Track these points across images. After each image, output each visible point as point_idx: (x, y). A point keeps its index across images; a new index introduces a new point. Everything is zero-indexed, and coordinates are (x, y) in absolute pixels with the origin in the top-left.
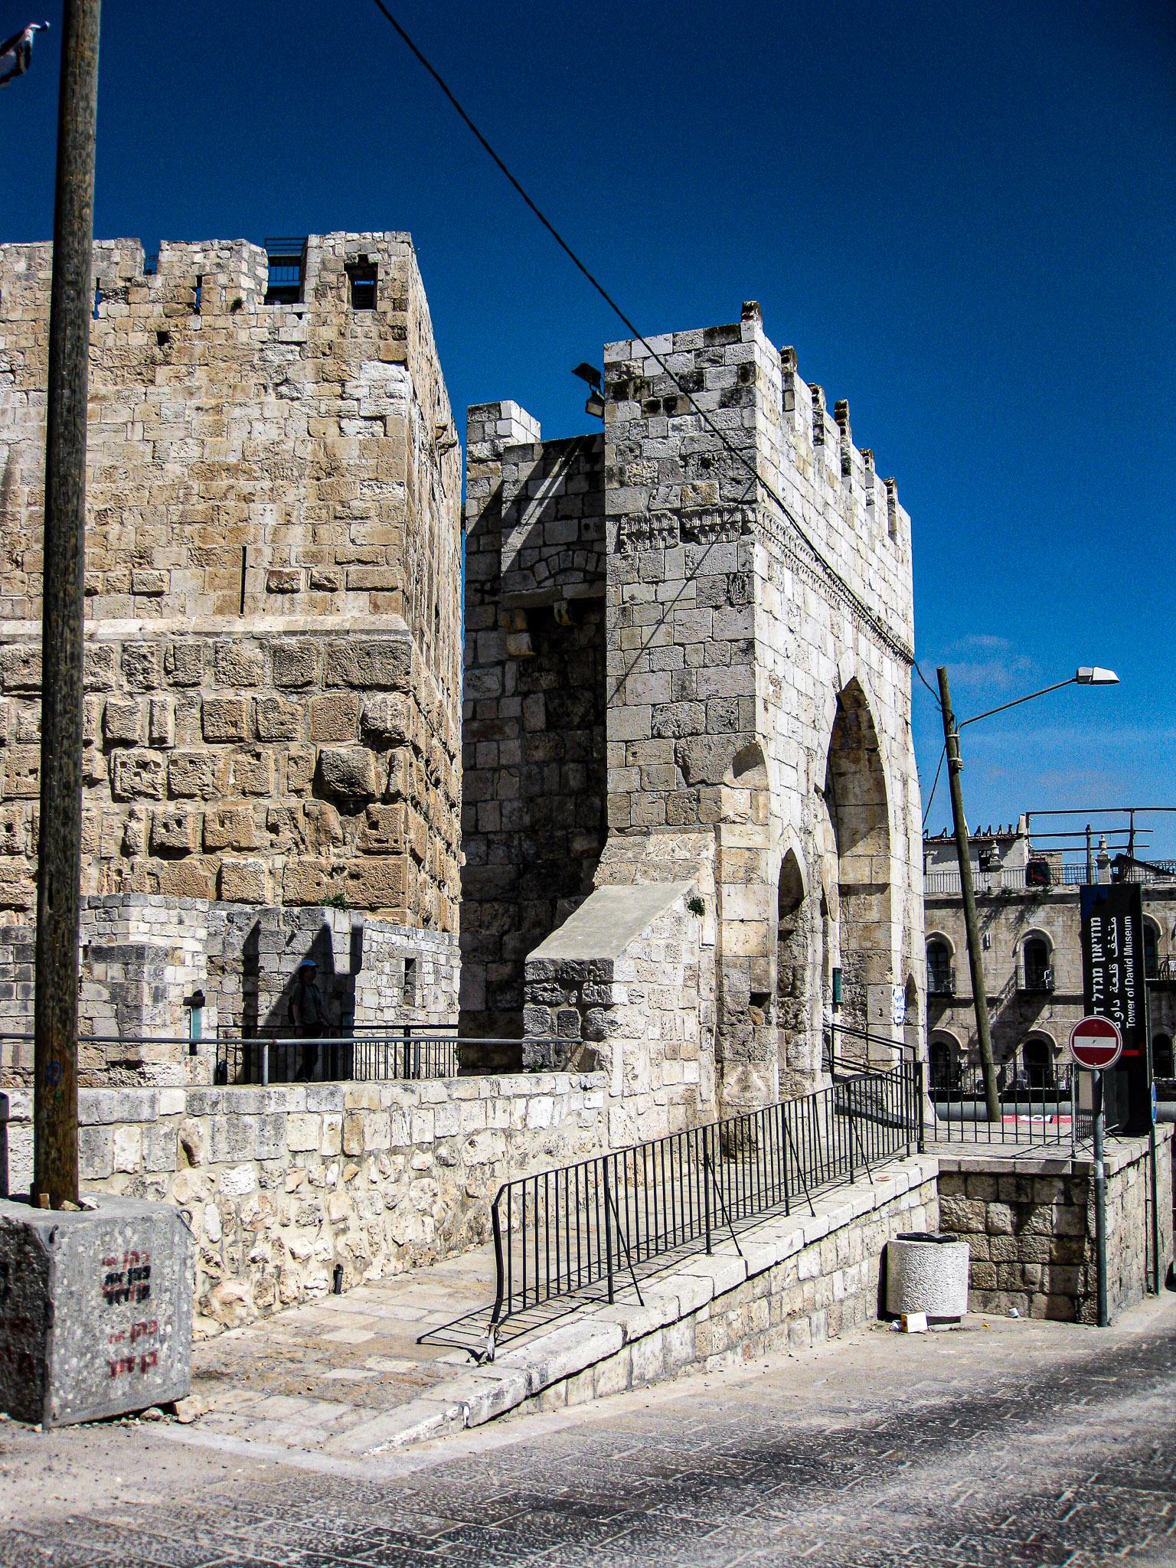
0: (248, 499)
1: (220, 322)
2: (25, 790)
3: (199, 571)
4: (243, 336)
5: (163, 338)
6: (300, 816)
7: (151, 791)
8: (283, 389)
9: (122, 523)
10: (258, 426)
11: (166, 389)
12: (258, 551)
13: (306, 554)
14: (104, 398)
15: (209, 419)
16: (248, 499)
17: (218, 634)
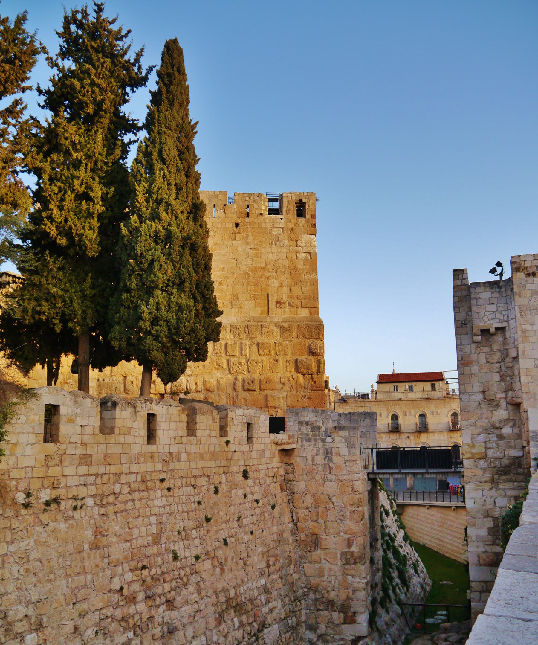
0: (268, 278)
1: (256, 221)
2: (201, 371)
3: (253, 301)
4: (264, 225)
5: (237, 225)
6: (291, 379)
7: (243, 372)
8: (278, 243)
9: (227, 286)
10: (270, 255)
11: (240, 242)
12: (272, 295)
13: (288, 296)
14: (219, 244)
15: (254, 252)
16: (268, 278)
17: (262, 322)
